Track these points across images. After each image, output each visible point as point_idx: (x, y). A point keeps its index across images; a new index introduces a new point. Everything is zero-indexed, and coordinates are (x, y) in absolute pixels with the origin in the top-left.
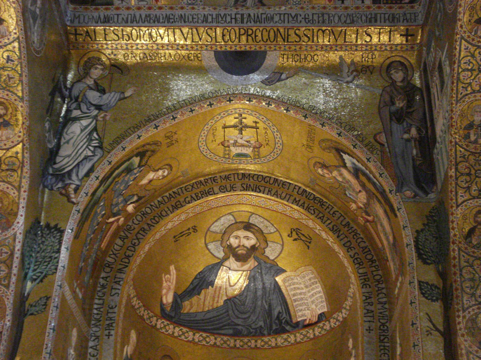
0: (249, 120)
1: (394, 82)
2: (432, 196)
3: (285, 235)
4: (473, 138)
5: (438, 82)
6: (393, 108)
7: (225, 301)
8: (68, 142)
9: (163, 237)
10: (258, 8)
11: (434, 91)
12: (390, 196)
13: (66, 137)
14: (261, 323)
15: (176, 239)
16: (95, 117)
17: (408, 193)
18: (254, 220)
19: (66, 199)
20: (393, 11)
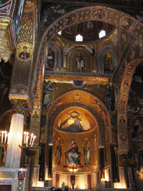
0: (79, 94)
1: (107, 88)
2: (114, 112)
3: (83, 114)
4: (122, 103)
5: (116, 91)
6: (107, 94)
7: (70, 126)
8: (45, 98)
9: (60, 115)
11: (115, 92)
12: (107, 112)
13: (45, 97)
14: (76, 130)
15: (62, 115)
16: (50, 93)
17: (110, 111)
18: (77, 111)
19: (46, 111)
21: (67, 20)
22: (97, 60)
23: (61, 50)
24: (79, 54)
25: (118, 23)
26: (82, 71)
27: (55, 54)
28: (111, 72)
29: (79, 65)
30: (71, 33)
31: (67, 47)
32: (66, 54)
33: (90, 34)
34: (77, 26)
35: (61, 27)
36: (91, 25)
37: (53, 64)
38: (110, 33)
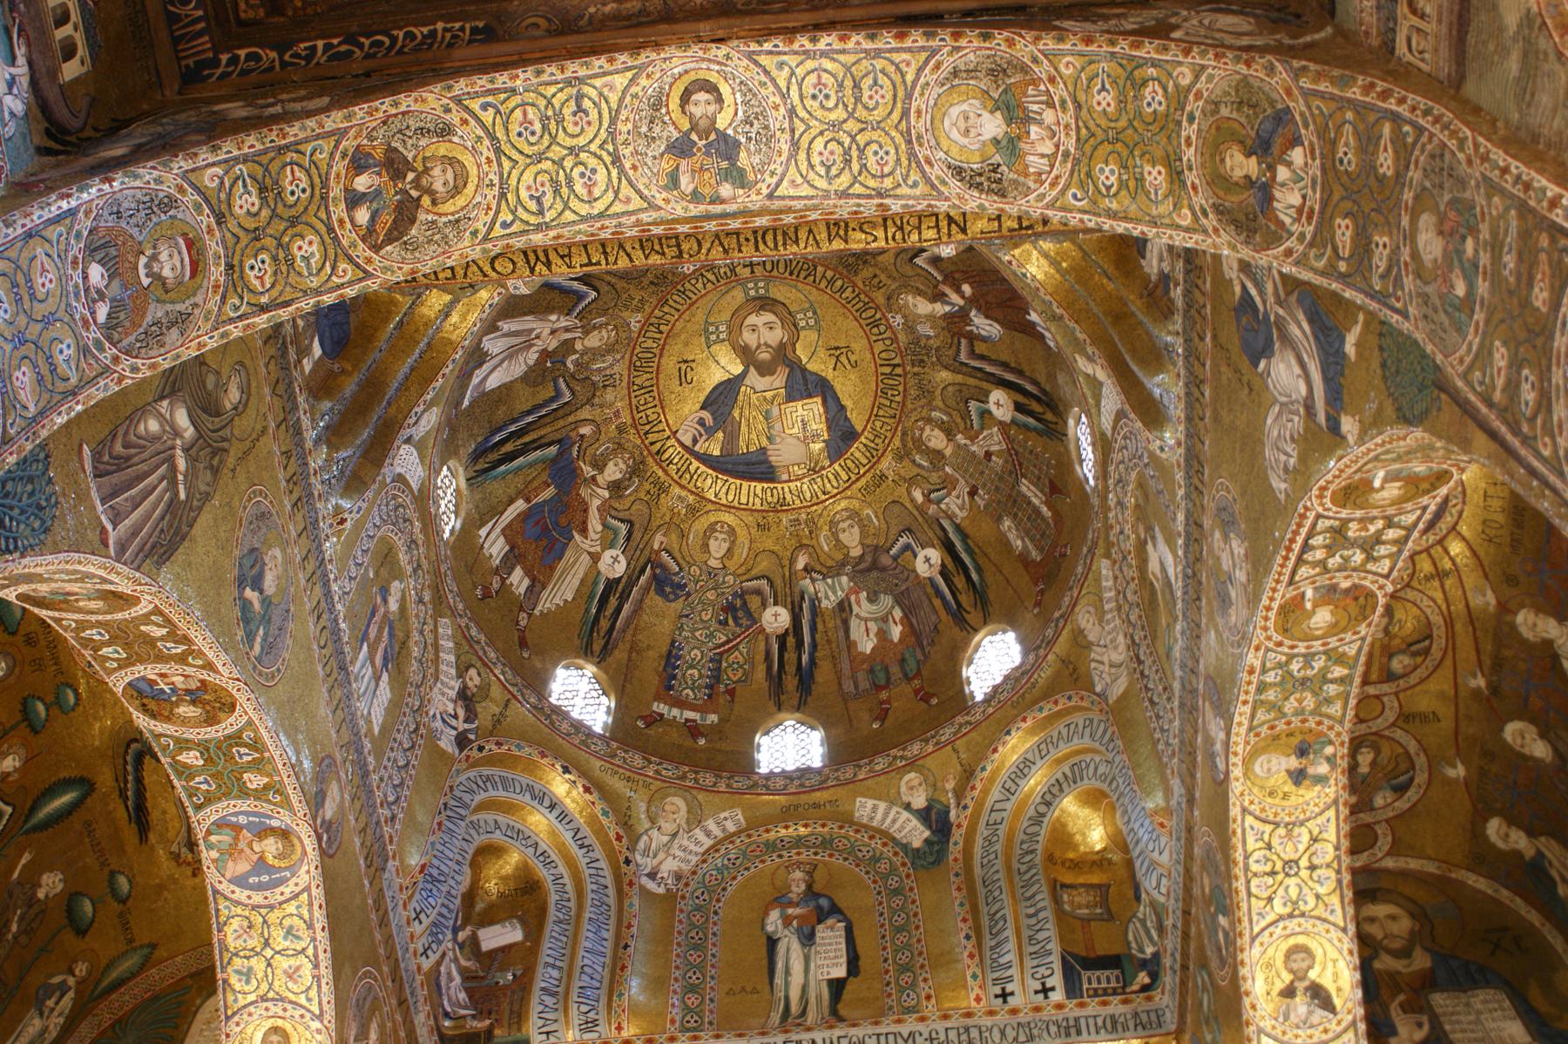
10: (831, 1027)
20: (1110, 1010)
21: (362, 183)
22: (981, 891)
23: (611, 855)
24: (798, 875)
25: (912, 155)
26: (835, 1016)
27: (553, 898)
28: (1143, 978)
29: (797, 966)
30: (713, 718)
31: (669, 827)
32: (661, 890)
33: (884, 695)
34: (760, 656)
35: (308, 248)
36: (884, 619)
37: (523, 985)
38: (1057, 615)
